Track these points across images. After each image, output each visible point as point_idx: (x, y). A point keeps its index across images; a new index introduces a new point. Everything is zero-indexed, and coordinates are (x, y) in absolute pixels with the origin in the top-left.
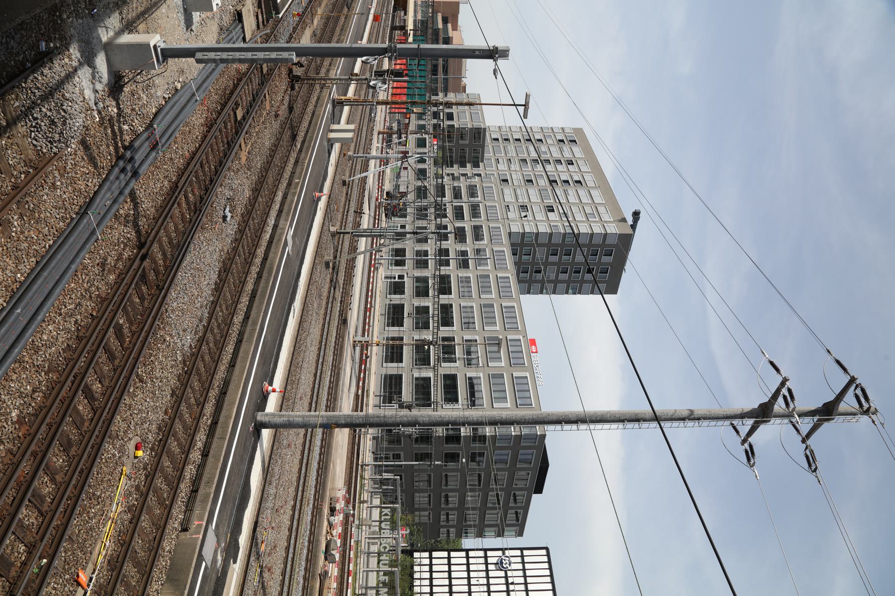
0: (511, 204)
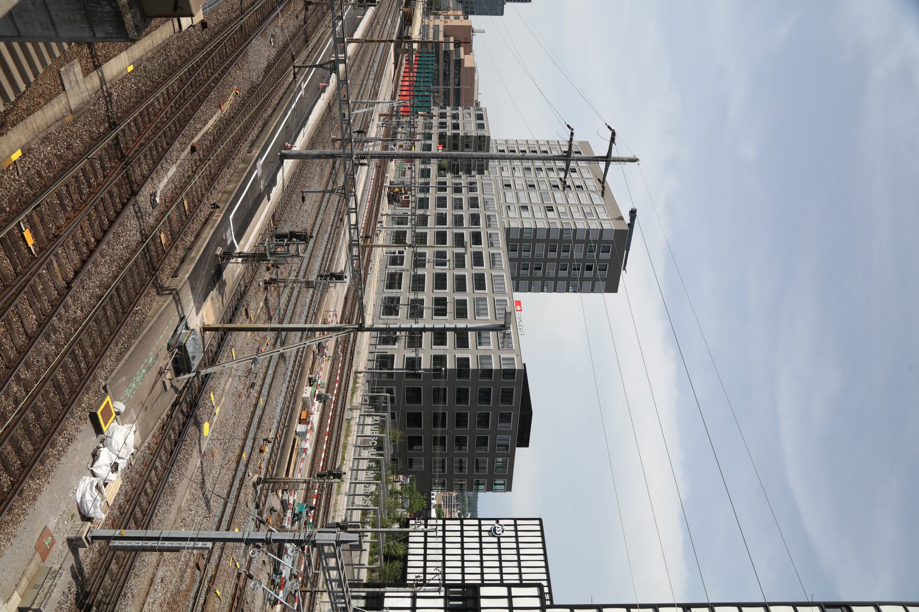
0: (512, 203)
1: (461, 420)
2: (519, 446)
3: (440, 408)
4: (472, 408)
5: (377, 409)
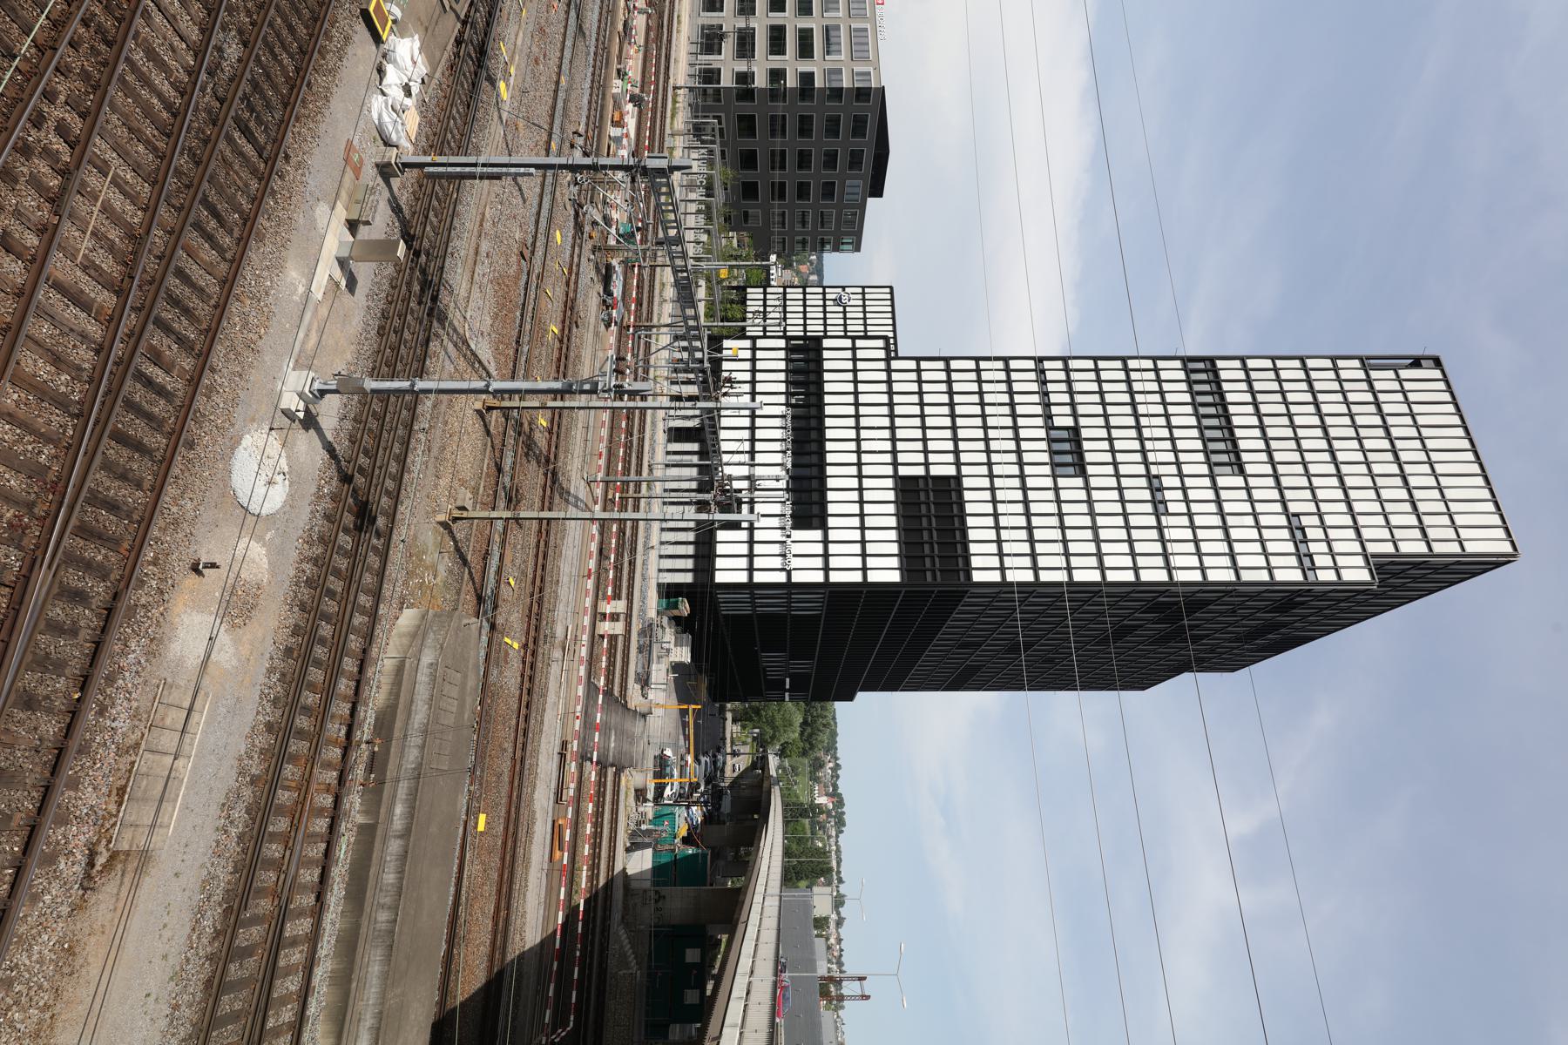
1: (804, 160)
2: (872, 195)
3: (778, 143)
4: (817, 144)
5: (703, 142)
